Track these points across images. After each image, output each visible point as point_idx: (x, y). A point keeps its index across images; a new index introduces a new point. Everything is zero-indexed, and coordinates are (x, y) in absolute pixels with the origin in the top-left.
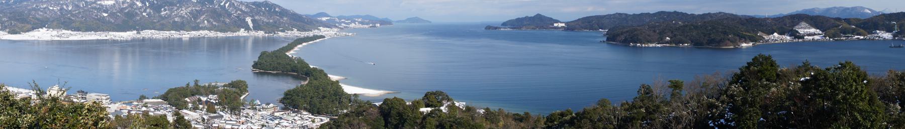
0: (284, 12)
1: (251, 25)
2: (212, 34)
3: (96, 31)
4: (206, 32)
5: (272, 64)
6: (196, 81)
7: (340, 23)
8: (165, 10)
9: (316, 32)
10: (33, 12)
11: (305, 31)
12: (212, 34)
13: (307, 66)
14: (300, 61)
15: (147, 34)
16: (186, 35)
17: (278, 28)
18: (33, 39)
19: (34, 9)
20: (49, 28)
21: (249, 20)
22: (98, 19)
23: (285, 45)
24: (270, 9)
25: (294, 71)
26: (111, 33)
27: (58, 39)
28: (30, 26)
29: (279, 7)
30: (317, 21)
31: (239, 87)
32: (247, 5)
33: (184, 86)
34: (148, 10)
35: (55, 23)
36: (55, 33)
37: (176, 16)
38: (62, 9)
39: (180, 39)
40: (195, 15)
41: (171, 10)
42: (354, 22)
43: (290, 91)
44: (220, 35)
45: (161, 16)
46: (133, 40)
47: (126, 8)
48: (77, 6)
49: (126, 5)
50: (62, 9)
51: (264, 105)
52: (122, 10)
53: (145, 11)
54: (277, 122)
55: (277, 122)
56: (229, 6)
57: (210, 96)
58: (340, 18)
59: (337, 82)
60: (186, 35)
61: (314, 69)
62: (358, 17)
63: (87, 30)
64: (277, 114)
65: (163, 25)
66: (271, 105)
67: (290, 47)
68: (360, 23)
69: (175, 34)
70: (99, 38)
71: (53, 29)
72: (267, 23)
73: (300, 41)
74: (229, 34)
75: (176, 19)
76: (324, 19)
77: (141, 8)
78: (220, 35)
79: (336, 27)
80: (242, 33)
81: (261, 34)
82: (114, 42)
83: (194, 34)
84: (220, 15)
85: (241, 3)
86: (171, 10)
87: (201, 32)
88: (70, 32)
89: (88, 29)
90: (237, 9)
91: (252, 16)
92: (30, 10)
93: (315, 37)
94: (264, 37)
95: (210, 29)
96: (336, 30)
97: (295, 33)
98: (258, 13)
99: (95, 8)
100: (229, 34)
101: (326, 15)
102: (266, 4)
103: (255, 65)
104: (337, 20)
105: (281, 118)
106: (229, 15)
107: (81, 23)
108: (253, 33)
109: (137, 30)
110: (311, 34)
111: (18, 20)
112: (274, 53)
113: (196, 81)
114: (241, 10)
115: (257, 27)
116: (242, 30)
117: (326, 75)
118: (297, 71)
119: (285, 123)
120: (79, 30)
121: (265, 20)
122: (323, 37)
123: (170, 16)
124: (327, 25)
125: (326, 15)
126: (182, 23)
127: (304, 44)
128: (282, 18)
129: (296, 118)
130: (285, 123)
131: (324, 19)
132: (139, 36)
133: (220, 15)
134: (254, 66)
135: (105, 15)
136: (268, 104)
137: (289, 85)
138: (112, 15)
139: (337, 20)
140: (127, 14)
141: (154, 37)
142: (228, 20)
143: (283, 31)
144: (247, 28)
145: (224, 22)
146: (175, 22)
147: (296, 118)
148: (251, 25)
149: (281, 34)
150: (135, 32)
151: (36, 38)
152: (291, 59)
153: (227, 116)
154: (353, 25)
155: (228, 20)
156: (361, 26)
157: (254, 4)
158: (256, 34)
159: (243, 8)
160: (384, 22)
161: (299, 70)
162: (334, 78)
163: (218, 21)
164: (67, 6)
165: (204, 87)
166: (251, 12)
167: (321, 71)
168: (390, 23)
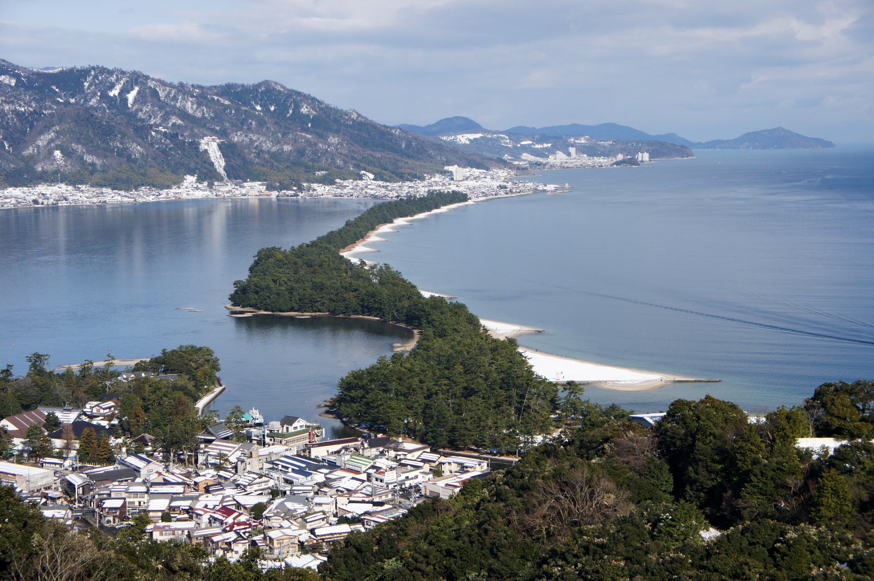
0: (328, 119)
2: (84, 196)
4: (62, 189)
11: (402, 178)
12: (84, 196)
17: (309, 170)
21: (211, 146)
29: (312, 101)
30: (441, 148)
32: (203, 95)
58: (516, 134)
62: (578, 130)
68: (581, 149)
72: (275, 156)
74: (146, 196)
78: (112, 197)
79: (503, 163)
80: (190, 189)
84: (106, 131)
85: (181, 88)
87: (42, 188)
90: (167, 109)
91: (222, 134)
95: (74, 180)
96: (502, 173)
98: (241, 124)
102: (267, 93)
106: (142, 130)
108: (226, 189)
110: (421, 189)
114: (183, 114)
115: (239, 170)
116: (190, 179)
121: (268, 145)
128: (322, 137)
133: (106, 131)
142: (137, 149)
143: (327, 181)
144: (207, 174)
145: (125, 154)
154: (559, 158)
155: (137, 149)
157: (227, 90)
158: (238, 192)
159: (190, 106)
163: (105, 152)
166: (218, 118)
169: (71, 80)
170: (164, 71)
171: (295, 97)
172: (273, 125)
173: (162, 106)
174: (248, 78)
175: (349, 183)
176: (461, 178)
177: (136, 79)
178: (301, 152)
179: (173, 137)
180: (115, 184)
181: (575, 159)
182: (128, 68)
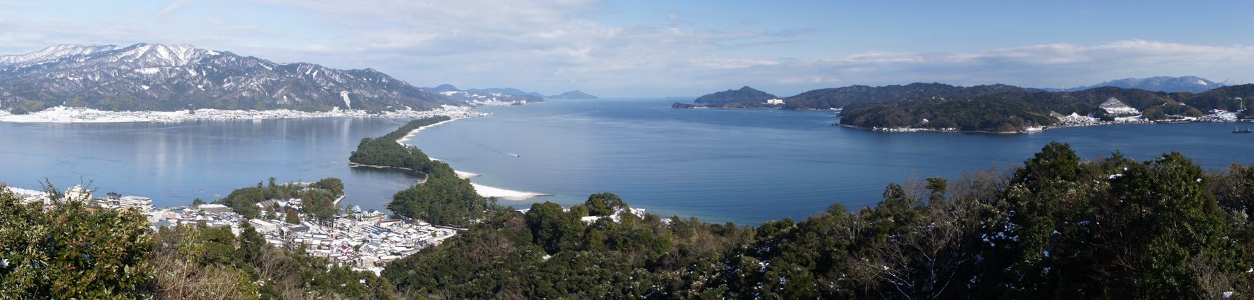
0: (393, 84)
1: (348, 102)
2: (294, 114)
3: (133, 110)
4: (286, 111)
5: (376, 156)
6: (272, 180)
7: (471, 99)
8: (229, 81)
9: (438, 112)
10: (46, 84)
11: (423, 109)
12: (294, 114)
13: (425, 158)
14: (416, 152)
15: (203, 114)
16: (257, 116)
18: (46, 121)
19: (47, 80)
20: (67, 106)
21: (345, 95)
22: (136, 94)
23: (395, 129)
24: (375, 80)
25: (407, 165)
26: (154, 113)
27: (81, 121)
28: (41, 103)
29: (386, 76)
30: (440, 97)
31: (331, 187)
32: (343, 74)
33: (255, 186)
34: (205, 82)
35: (76, 100)
36: (76, 112)
37: (244, 89)
38: (85, 80)
39: (250, 122)
40: (271, 88)
41: (237, 82)
42: (491, 97)
43: (401, 193)
44: (305, 115)
45: (223, 90)
46: (185, 123)
47: (175, 78)
48: (107, 76)
49: (174, 74)
50: (85, 80)
51: (366, 213)
52: (169, 81)
53: (201, 83)
54: (383, 235)
55: (383, 235)
56: (318, 75)
57: (292, 200)
58: (471, 92)
59: (468, 180)
60: (257, 116)
61: (436, 163)
62: (497, 90)
63: (120, 109)
64: (383, 225)
65: (226, 101)
66: (376, 213)
67: (402, 132)
68: (498, 99)
69: (242, 115)
70: (138, 120)
71: (74, 107)
73: (415, 124)
74: (318, 115)
75: (244, 94)
76: (449, 93)
77: (196, 78)
78: (305, 115)
79: (465, 104)
80: (335, 112)
81: (361, 114)
82: (158, 125)
83: (269, 114)
84: (304, 88)
85: (334, 71)
86: (237, 82)
88: (97, 111)
89: (122, 107)
90: (328, 80)
91: (349, 90)
92: (41, 82)
93: (437, 119)
94: (365, 119)
95: (291, 108)
96: (465, 108)
97: (409, 113)
98: (357, 86)
99: (132, 79)
100: (318, 115)
101: (452, 88)
102: (368, 73)
103: (354, 158)
104: (467, 95)
105: (389, 231)
106: (318, 88)
107: (113, 98)
109: (190, 109)
110: (431, 114)
111: (24, 95)
112: (380, 140)
113: (272, 180)
114: (334, 81)
115: (356, 105)
116: (336, 108)
117: (451, 171)
118: (411, 166)
119: (395, 238)
120: (109, 109)
121: (368, 95)
122: (448, 118)
123: (235, 89)
124: (454, 102)
125: (452, 88)
126: (253, 99)
127: (422, 128)
129: (410, 230)
130: (395, 238)
131: (449, 93)
132: (192, 117)
133: (304, 88)
134: (352, 159)
135: (146, 88)
136: (371, 211)
137: (400, 184)
138: (155, 88)
139: (467, 95)
140: (176, 87)
141: (214, 118)
142: (315, 96)
143: (392, 110)
144: (343, 107)
145: (310, 98)
146: (242, 97)
147: (410, 230)
148: (348, 102)
149: (389, 114)
150: (187, 111)
151: (50, 120)
152: (403, 149)
153: (314, 228)
154: (489, 102)
155: (315, 96)
156: (500, 103)
157: (352, 72)
159: (337, 78)
160: (531, 98)
161: (414, 164)
162: (463, 175)
163: (303, 97)
164: (94, 76)
165: (283, 187)
166: (348, 83)
167: (445, 166)
168: (540, 99)
169: (292, 68)
170: (326, 64)
171: (379, 75)
172: (372, 87)
173: (326, 78)
174: (361, 67)
175: (401, 111)
176: (448, 110)
177: (317, 67)
178: (382, 98)
179: (330, 91)
180: (307, 110)
181: (496, 103)
182: (314, 63)
